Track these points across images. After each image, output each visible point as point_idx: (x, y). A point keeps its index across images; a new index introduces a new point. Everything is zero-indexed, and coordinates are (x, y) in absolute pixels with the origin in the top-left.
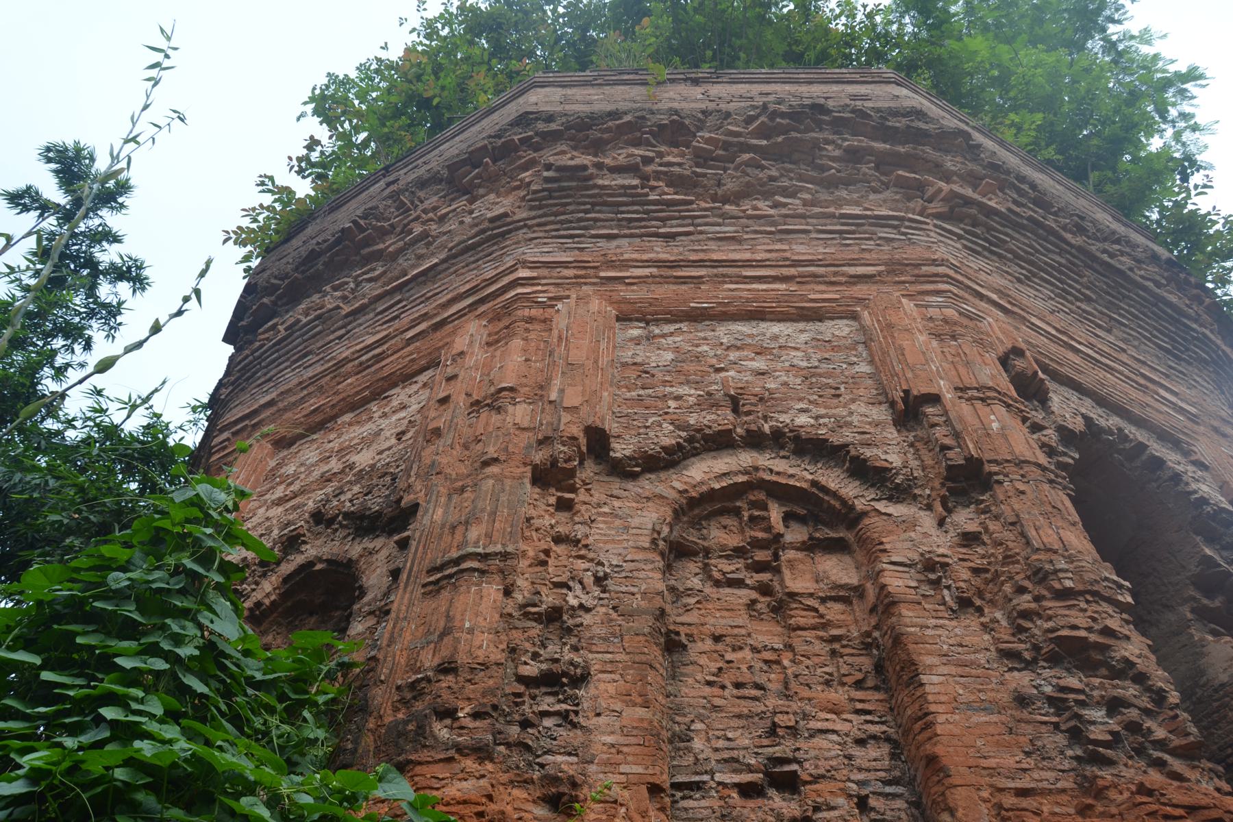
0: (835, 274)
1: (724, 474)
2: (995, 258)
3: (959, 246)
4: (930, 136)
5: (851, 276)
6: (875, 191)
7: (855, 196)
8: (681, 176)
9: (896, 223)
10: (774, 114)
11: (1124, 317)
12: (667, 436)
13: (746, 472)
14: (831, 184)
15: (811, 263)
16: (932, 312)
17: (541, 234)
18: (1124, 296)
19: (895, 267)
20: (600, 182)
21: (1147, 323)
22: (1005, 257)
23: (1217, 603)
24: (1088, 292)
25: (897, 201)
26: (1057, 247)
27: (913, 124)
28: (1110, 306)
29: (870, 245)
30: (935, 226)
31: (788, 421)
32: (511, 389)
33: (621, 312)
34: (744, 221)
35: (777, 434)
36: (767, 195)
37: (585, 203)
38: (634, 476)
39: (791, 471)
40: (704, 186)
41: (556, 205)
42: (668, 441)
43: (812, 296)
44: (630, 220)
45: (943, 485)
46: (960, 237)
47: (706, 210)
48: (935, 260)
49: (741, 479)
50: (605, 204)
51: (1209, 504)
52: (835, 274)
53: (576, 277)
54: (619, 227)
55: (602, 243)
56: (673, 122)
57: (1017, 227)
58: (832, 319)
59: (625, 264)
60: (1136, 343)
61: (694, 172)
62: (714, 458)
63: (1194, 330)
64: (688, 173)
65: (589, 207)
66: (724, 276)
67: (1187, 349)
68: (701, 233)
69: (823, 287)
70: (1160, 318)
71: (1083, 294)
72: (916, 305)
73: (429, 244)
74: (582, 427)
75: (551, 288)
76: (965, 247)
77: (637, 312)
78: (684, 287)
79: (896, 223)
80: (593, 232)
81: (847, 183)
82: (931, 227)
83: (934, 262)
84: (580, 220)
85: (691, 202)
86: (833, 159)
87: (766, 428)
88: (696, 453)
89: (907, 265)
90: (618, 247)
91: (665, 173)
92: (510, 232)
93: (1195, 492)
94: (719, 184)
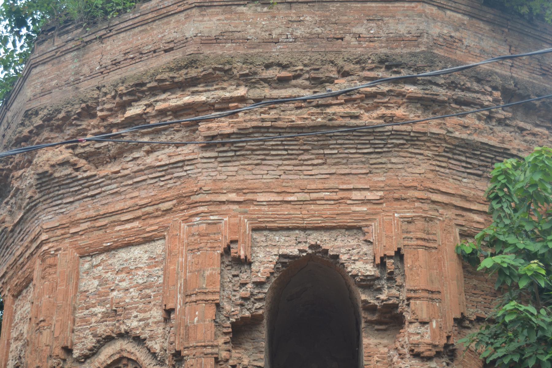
0: (157, 210)
1: (112, 355)
2: (241, 158)
3: (216, 164)
4: (199, 79)
5: (163, 211)
6: (178, 131)
7: (169, 138)
8: (91, 152)
9: (180, 164)
10: (121, 96)
11: (334, 149)
12: (90, 342)
13: (119, 353)
14: (158, 132)
15: (146, 205)
16: (194, 230)
17: (46, 206)
18: (331, 137)
19: (181, 198)
20: (57, 175)
21: (352, 144)
22: (246, 155)
23: (375, 318)
24: (305, 147)
25: (188, 136)
26: (277, 133)
27: (189, 76)
28: (323, 147)
29: (171, 184)
30: (201, 158)
31: (129, 325)
32: (44, 321)
33: (80, 254)
34: (119, 179)
35: (127, 332)
36: (131, 150)
37: (56, 187)
38: (83, 362)
39: (133, 350)
40: (103, 153)
41: (46, 189)
42: (90, 346)
43: (148, 230)
44: (76, 191)
45: (173, 359)
46: (216, 158)
47: (102, 178)
48: (196, 192)
49: (116, 357)
50: (63, 185)
51: (358, 276)
52: (157, 210)
53: (62, 234)
54: (73, 195)
55: (71, 207)
56: (82, 108)
57: (246, 135)
58: (158, 240)
59: (76, 223)
60: (345, 161)
61: (95, 148)
62: (109, 346)
63: (387, 132)
64: (93, 150)
65: (58, 188)
66: (114, 222)
67: (387, 144)
68: (104, 192)
69: (151, 221)
70: (360, 136)
71: (302, 150)
72: (188, 226)
73: (21, 193)
74: (60, 347)
75: (55, 244)
76: (220, 162)
77: (86, 252)
78: (101, 232)
79: (180, 164)
80: (65, 201)
81: (165, 130)
82: (199, 160)
83: (196, 193)
84: (58, 195)
85: (95, 175)
86: (154, 117)
87: (123, 331)
88: (102, 345)
89: (185, 197)
90: (75, 208)
91: (84, 153)
92: (36, 205)
93: (350, 272)
94: (109, 151)
